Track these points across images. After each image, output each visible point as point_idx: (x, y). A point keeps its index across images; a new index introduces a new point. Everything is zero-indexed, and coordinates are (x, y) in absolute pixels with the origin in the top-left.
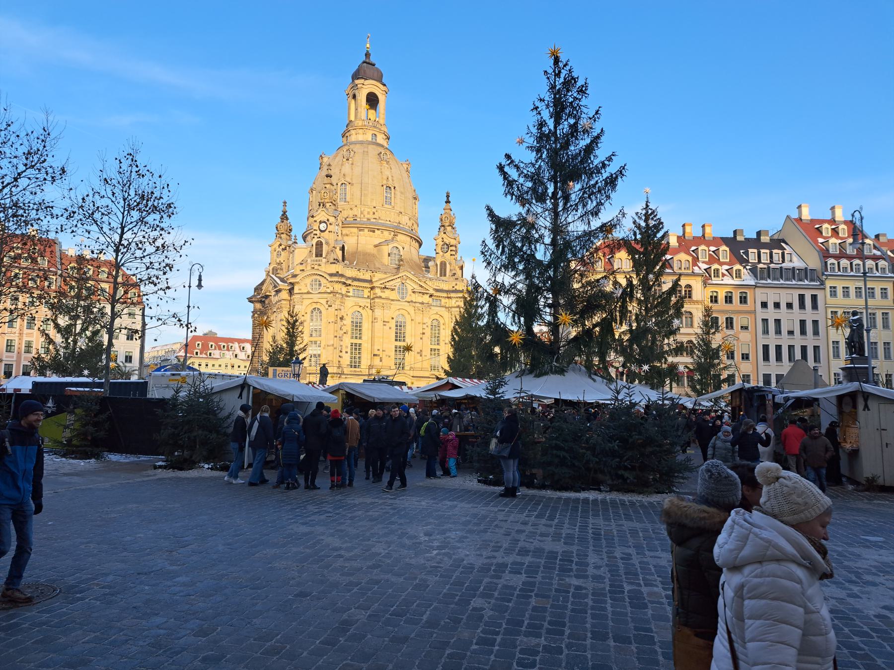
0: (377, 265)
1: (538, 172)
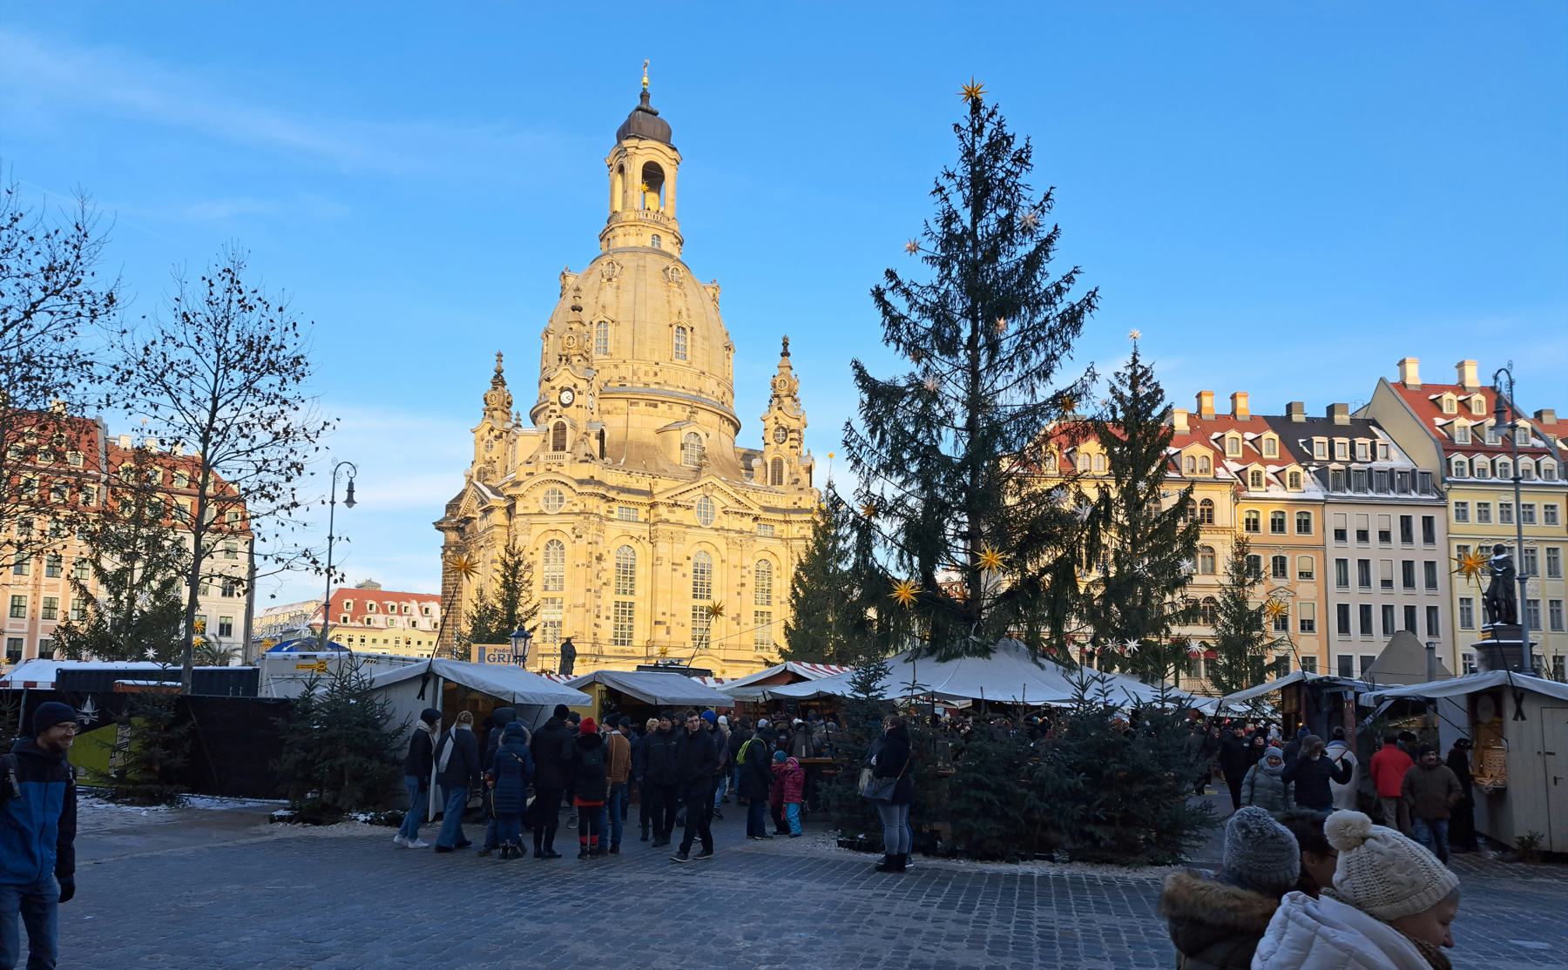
0: (662, 465)
1: (943, 302)
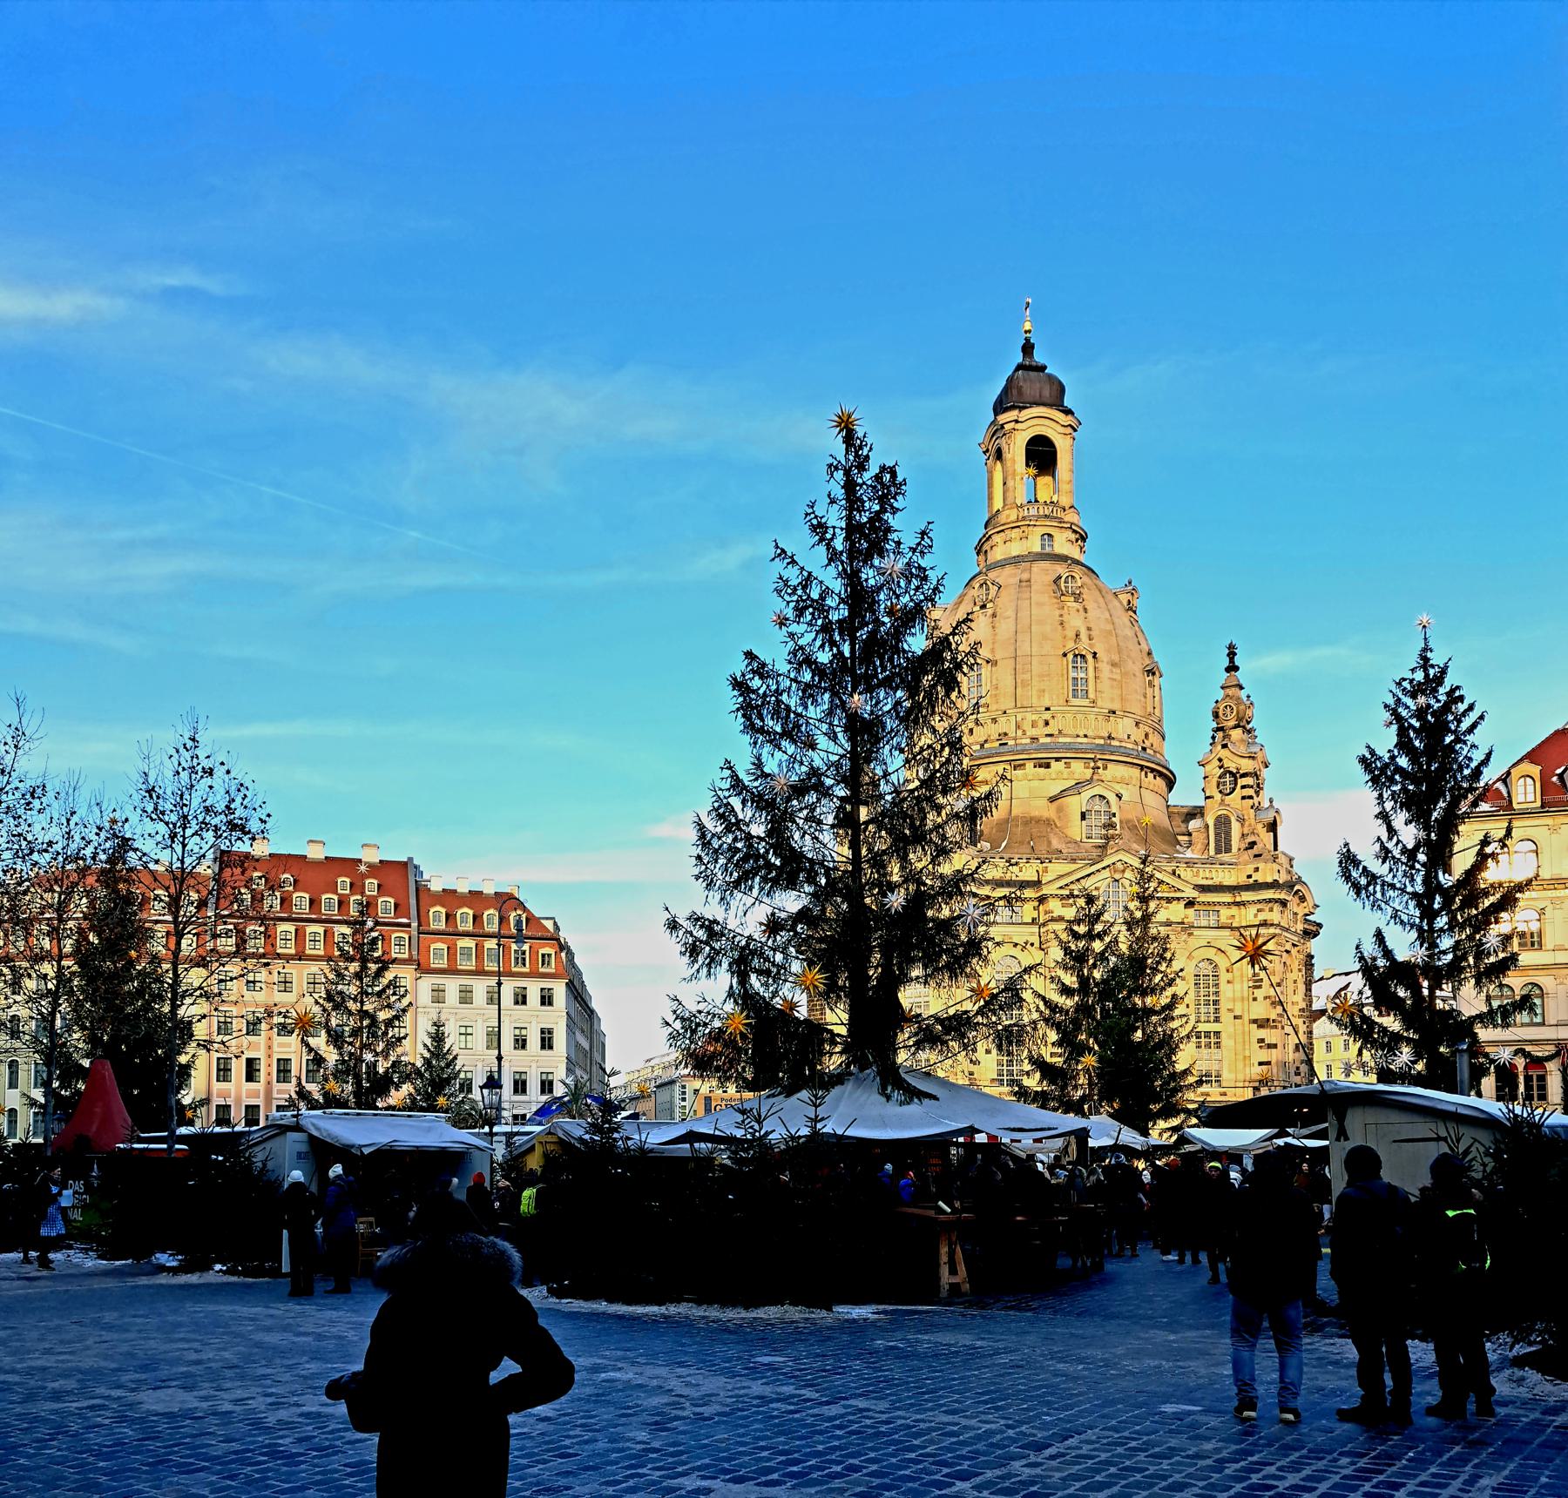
0: (1056, 843)
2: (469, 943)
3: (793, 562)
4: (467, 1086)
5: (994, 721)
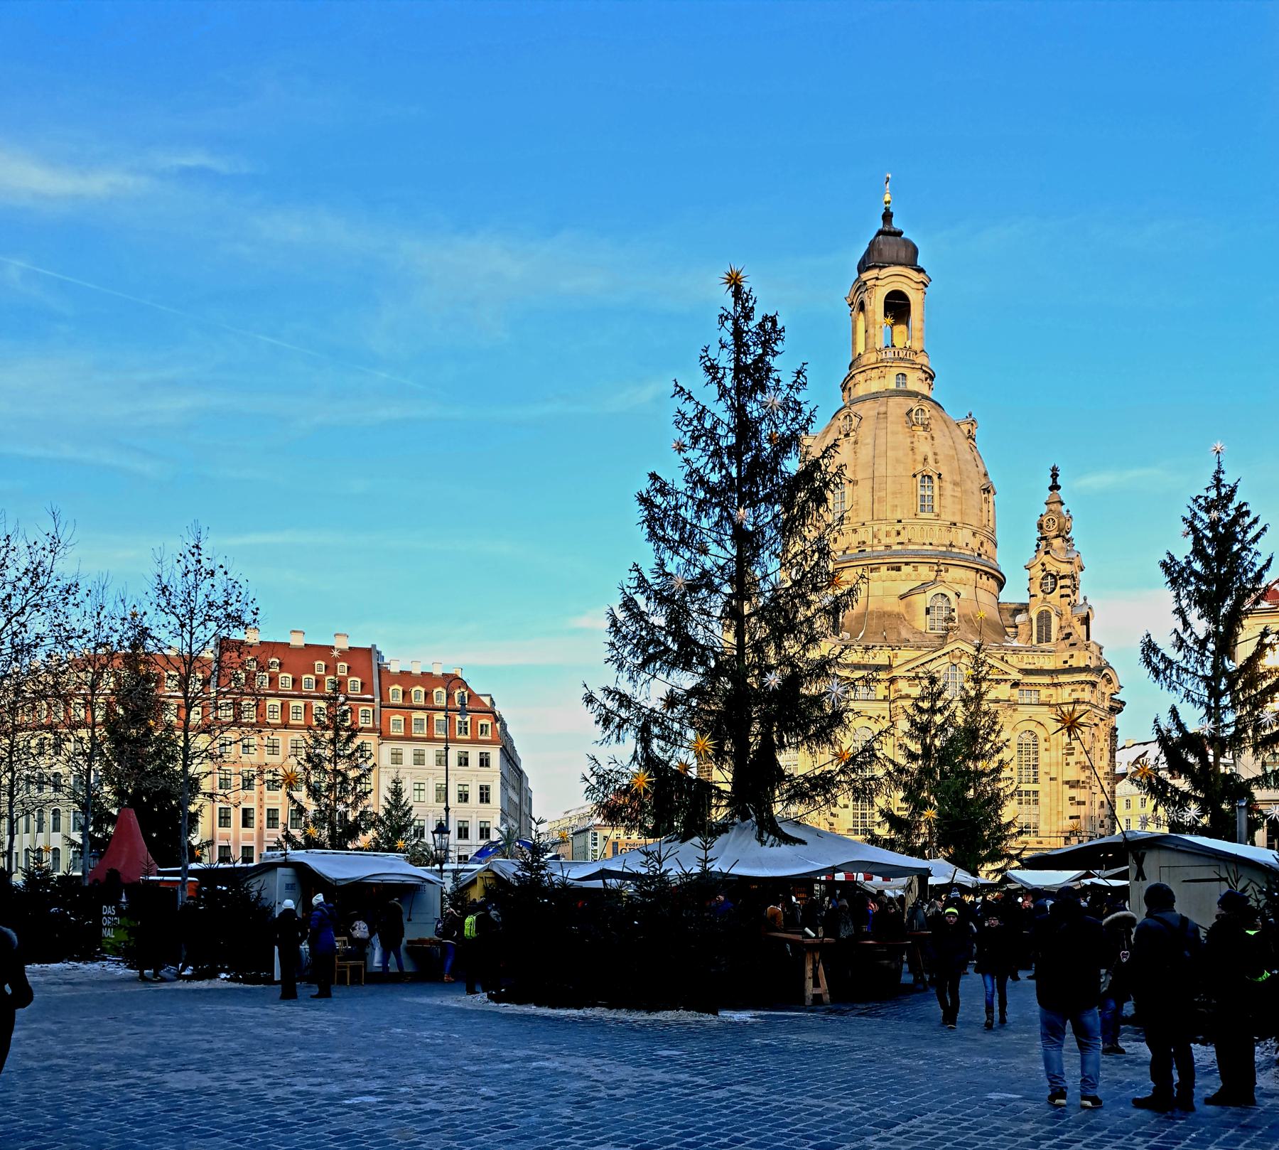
2: (422, 715)
3: (690, 398)
4: (420, 832)
5: (855, 531)
